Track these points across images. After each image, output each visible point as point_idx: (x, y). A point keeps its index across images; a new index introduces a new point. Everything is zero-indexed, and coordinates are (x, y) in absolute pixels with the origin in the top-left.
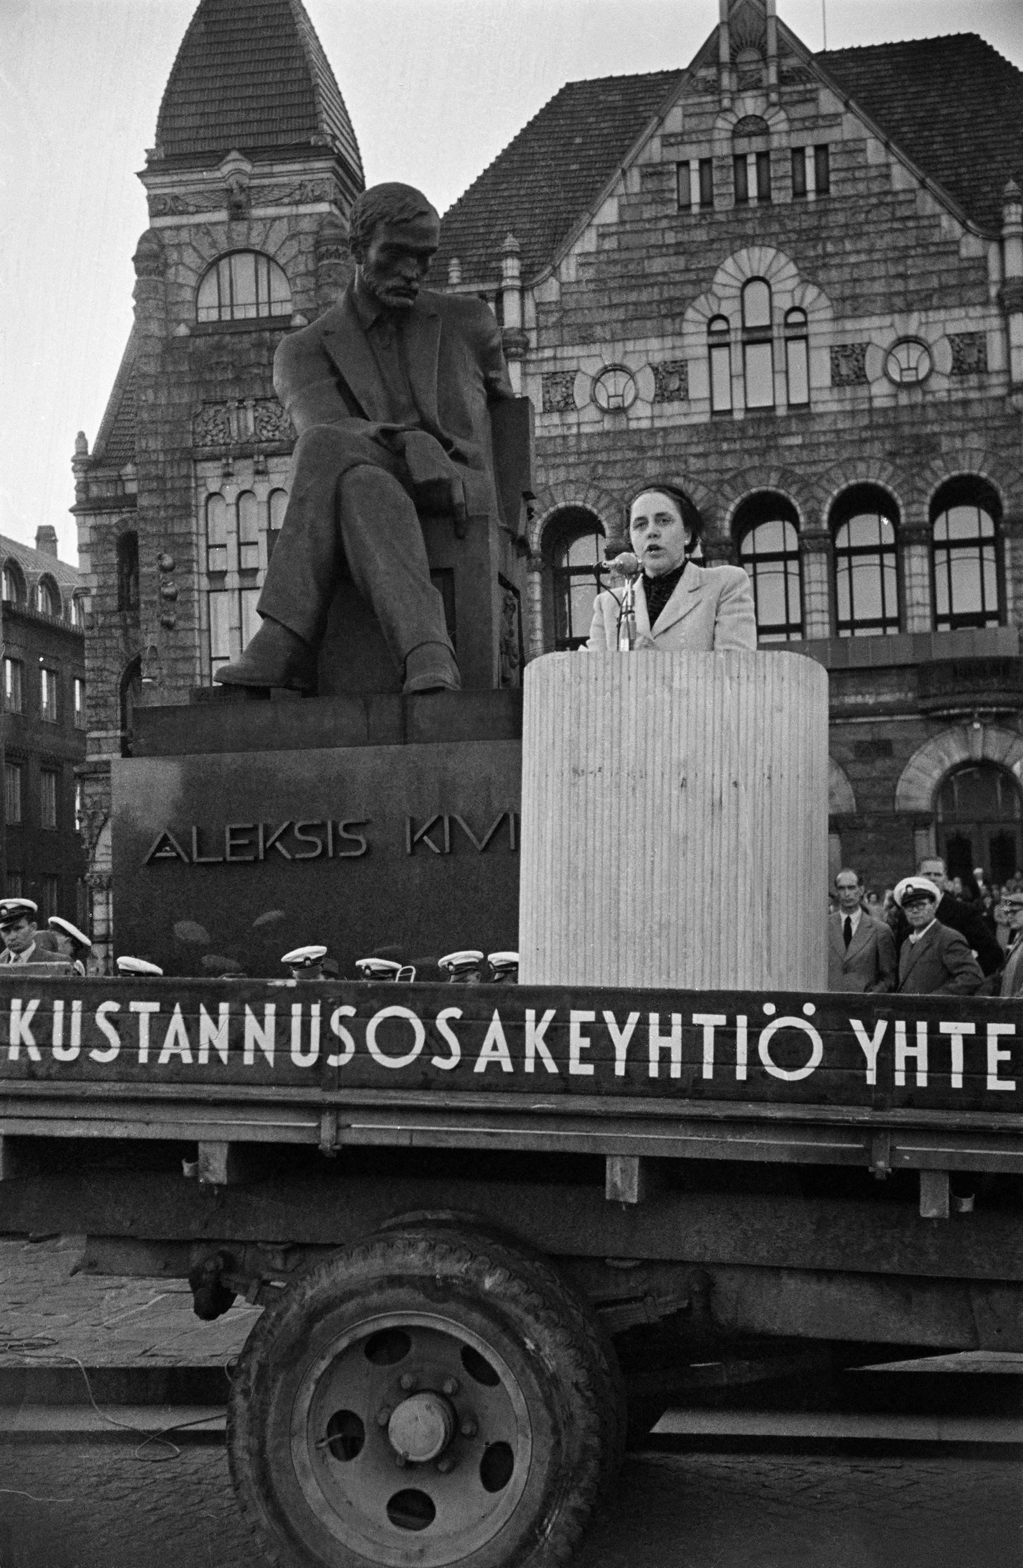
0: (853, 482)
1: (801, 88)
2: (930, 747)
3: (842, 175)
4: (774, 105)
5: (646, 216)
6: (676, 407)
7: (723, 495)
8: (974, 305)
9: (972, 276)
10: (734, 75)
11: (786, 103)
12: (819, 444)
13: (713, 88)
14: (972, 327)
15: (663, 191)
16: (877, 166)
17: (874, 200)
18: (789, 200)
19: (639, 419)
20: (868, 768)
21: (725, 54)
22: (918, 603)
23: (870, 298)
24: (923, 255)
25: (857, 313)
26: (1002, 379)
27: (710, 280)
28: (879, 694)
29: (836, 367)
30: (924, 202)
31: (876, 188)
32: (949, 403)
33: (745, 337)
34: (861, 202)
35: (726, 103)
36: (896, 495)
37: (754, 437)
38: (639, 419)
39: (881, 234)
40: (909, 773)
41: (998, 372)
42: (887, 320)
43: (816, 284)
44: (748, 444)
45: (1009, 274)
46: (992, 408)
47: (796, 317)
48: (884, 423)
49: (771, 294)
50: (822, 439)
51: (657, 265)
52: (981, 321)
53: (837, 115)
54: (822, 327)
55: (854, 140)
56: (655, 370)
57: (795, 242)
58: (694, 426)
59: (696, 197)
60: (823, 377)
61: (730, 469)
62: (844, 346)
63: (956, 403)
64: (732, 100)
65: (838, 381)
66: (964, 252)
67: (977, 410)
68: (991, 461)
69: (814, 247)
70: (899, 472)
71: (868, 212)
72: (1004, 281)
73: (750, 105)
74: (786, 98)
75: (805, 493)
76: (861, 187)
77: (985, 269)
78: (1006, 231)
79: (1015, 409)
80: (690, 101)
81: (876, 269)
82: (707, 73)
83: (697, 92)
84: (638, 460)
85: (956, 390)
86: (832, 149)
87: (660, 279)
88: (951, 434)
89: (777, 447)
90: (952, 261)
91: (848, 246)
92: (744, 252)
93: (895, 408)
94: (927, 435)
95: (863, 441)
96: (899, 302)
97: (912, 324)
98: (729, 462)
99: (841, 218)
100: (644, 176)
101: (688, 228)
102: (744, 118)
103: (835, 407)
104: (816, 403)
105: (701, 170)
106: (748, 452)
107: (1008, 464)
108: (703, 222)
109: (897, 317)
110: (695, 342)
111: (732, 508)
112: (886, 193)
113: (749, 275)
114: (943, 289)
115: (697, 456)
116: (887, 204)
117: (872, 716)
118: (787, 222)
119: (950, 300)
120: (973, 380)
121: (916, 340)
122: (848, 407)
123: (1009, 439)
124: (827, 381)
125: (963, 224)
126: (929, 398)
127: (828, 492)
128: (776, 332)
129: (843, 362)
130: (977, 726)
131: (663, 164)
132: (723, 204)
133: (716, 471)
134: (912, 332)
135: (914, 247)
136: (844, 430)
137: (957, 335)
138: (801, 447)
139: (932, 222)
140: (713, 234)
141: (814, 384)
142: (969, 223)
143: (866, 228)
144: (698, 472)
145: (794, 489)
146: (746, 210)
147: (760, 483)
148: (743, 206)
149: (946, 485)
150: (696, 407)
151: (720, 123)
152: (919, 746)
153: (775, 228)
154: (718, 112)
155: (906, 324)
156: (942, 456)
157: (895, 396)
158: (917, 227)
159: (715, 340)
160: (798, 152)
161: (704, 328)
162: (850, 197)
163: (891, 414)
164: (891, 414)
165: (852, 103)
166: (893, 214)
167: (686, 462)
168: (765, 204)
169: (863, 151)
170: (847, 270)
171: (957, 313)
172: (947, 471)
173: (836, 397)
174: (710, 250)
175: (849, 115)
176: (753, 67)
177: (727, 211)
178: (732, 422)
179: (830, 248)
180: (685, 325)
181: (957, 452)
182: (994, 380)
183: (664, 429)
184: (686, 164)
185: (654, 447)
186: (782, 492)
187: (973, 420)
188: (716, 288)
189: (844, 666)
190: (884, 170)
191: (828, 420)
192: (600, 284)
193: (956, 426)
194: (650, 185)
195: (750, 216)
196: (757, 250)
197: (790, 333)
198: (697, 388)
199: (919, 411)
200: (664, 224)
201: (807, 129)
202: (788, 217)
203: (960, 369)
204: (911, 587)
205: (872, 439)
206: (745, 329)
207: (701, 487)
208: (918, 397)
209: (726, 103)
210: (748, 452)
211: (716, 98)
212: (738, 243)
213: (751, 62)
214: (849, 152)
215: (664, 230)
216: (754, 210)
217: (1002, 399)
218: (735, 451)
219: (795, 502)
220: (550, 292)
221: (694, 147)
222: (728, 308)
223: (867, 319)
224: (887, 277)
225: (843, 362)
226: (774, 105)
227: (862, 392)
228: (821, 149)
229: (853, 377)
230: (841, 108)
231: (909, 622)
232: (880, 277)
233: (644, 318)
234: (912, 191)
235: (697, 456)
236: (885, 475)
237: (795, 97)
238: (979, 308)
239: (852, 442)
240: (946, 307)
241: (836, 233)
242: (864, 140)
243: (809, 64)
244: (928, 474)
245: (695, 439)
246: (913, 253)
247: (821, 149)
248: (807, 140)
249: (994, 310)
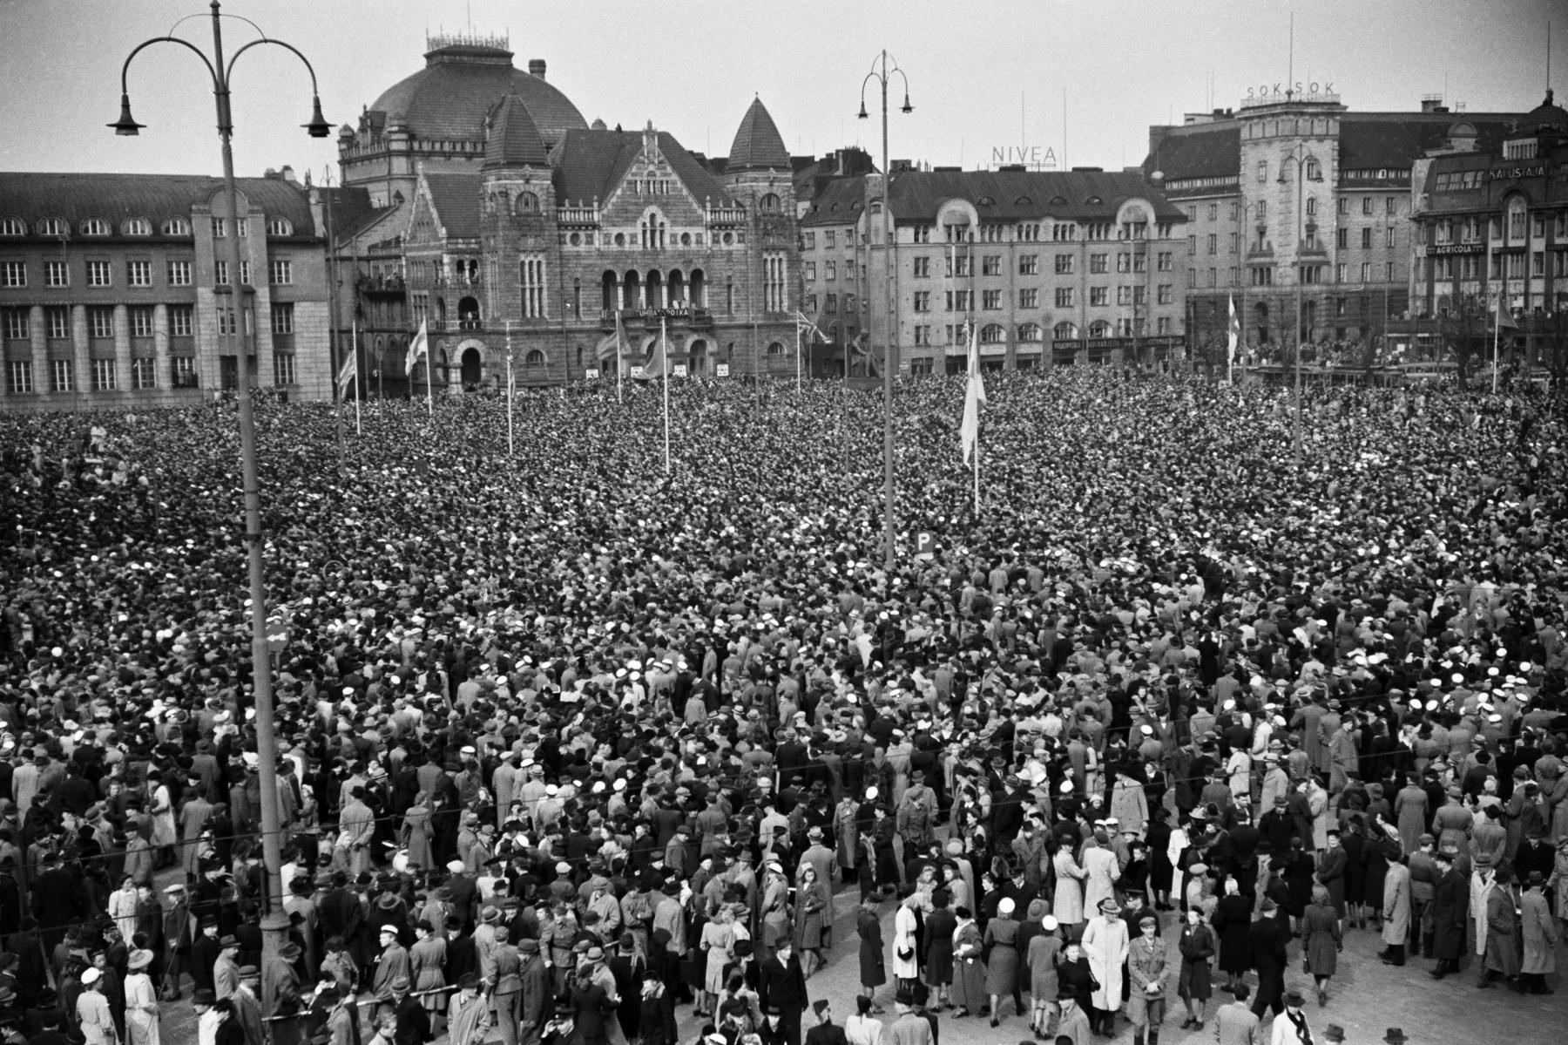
73: (652, 168)
192: (617, 211)
220: (605, 212)
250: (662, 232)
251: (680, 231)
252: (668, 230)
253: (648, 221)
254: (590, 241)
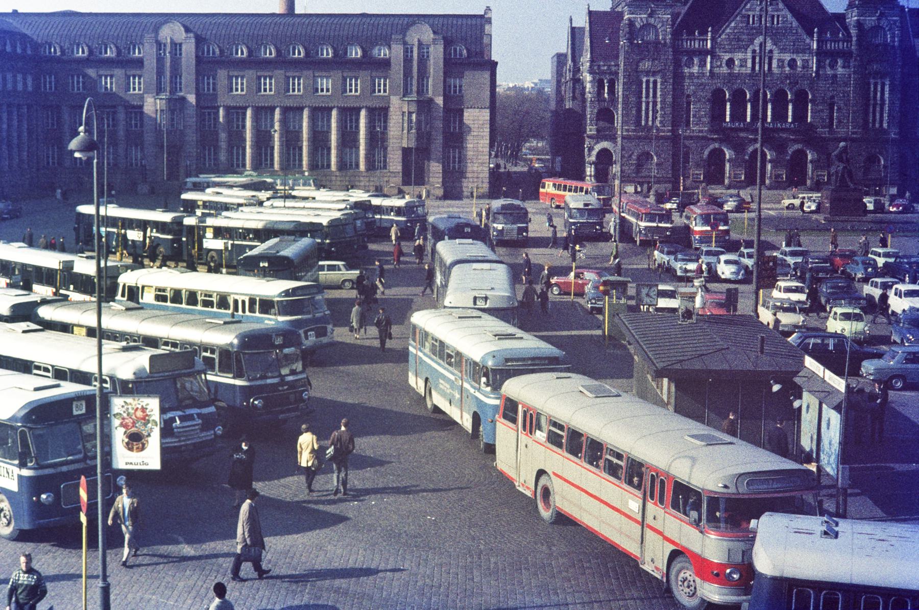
48: (787, 77)
65: (778, 66)
97: (795, 56)
228: (778, 16)
250: (770, 59)
251: (787, 57)
252: (776, 55)
253: (757, 49)
254: (703, 64)
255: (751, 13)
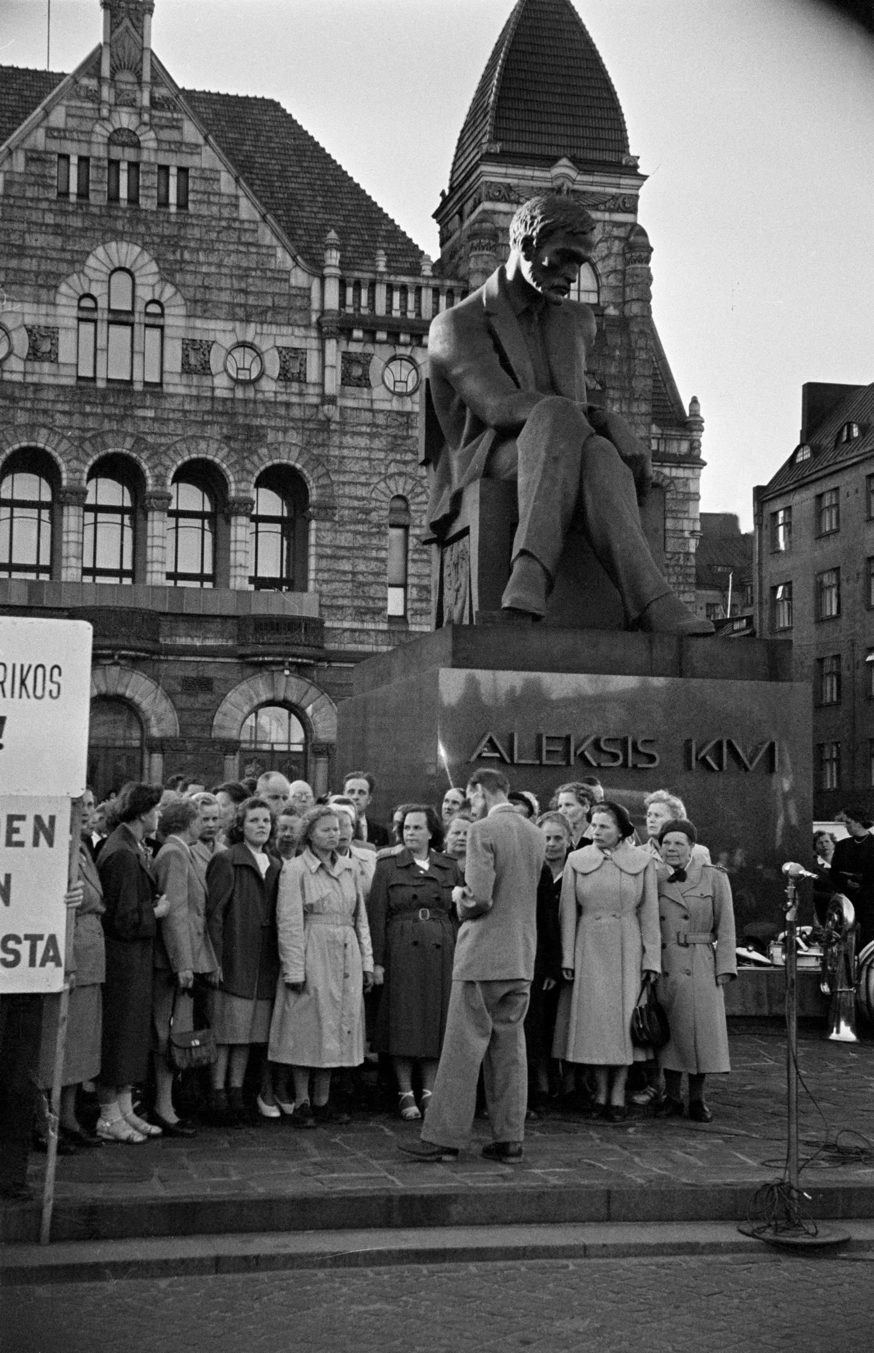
0: (194, 456)
1: (169, 115)
2: (244, 687)
3: (199, 196)
4: (145, 124)
5: (29, 194)
6: (46, 367)
7: (84, 450)
8: (299, 326)
9: (299, 303)
10: (113, 91)
11: (156, 125)
12: (168, 420)
13: (95, 97)
14: (296, 344)
15: (44, 176)
16: (229, 196)
17: (224, 223)
18: (154, 208)
19: (11, 372)
20: (192, 699)
21: (106, 71)
22: (241, 566)
23: (218, 304)
24: (262, 278)
25: (207, 315)
26: (317, 390)
27: (83, 263)
28: (205, 638)
29: (186, 357)
30: (264, 234)
31: (226, 213)
32: (275, 403)
33: (111, 317)
34: (214, 223)
35: (105, 113)
36: (229, 472)
37: (114, 405)
38: (11, 372)
39: (229, 253)
40: (225, 706)
41: (314, 384)
42: (229, 326)
43: (173, 284)
44: (108, 410)
45: (328, 306)
46: (309, 412)
47: (154, 309)
48: (224, 411)
49: (134, 285)
50: (171, 416)
51: (36, 240)
52: (304, 340)
53: (198, 146)
54: (176, 320)
55: (211, 170)
56: (30, 331)
57: (158, 245)
58: (62, 387)
59: (73, 188)
60: (174, 362)
61: (93, 429)
62: (194, 340)
63: (281, 403)
64: (110, 111)
65: (187, 369)
66: (293, 282)
67: (296, 412)
68: (306, 456)
69: (174, 252)
70: (233, 453)
71: (219, 232)
72: (323, 312)
73: (125, 119)
74: (156, 121)
75: (155, 460)
76: (215, 209)
77: (309, 298)
78: (327, 271)
79: (325, 415)
80: (73, 103)
81: (223, 281)
82: (92, 83)
83: (78, 96)
84: (9, 408)
85: (282, 393)
86: (191, 173)
87: (39, 252)
88: (276, 429)
89: (133, 417)
90: (284, 287)
91: (202, 257)
92: (113, 244)
93: (233, 400)
94: (257, 426)
95: (205, 423)
96: (240, 312)
97: (250, 333)
98: (91, 423)
99: (197, 232)
100: (29, 160)
101: (64, 213)
102: (119, 129)
103: (182, 390)
104: (168, 384)
105: (79, 166)
106: (109, 417)
107: (318, 461)
108: (80, 211)
109: (238, 324)
110: (66, 313)
111: (91, 463)
112: (235, 220)
113: (117, 265)
114: (275, 308)
115: (64, 413)
116: (235, 229)
117: (201, 656)
118: (153, 226)
119: (280, 318)
120: (295, 387)
121: (251, 346)
122: (194, 392)
123: (320, 440)
124: (179, 369)
125: (294, 258)
126: (260, 396)
127: (174, 461)
128: (137, 318)
129: (192, 354)
130: (287, 672)
131: (46, 152)
132: (98, 199)
133: (79, 429)
134: (249, 339)
135: (255, 270)
136: (190, 411)
137: (284, 348)
138: (154, 419)
139: (271, 252)
140: (87, 224)
141: (167, 367)
142: (299, 258)
143: (217, 246)
144: (64, 427)
145: (145, 455)
146: (118, 208)
147: (116, 445)
148: (114, 204)
149: (267, 470)
150: (64, 371)
151: (98, 128)
152: (235, 685)
153: (142, 229)
154: (97, 119)
155: (245, 332)
156: (268, 446)
157: (232, 390)
158: (258, 253)
159: (85, 315)
160: (164, 169)
161: (75, 303)
162: (204, 217)
163: (229, 404)
164: (229, 404)
165: (210, 138)
166: (239, 238)
167: (52, 417)
168: (134, 207)
169: (218, 180)
170: (200, 277)
171: (286, 330)
172: (271, 458)
173: (184, 382)
174: (84, 237)
175: (208, 148)
176: (129, 87)
177: (100, 206)
178: (96, 389)
179: (187, 256)
180: (58, 297)
181: (279, 443)
182: (312, 390)
183: (34, 384)
184: (65, 157)
185: (25, 399)
186: (135, 455)
187: (293, 420)
188: (87, 270)
189: (179, 612)
190: (234, 200)
191: (177, 401)
193: (279, 423)
194: (34, 168)
195: (120, 214)
196: (125, 245)
197: (150, 321)
198: (66, 354)
199: (251, 406)
200: (44, 205)
201: (172, 151)
202: (153, 222)
203: (285, 376)
204: (235, 552)
205: (212, 423)
206: (110, 311)
207: (65, 441)
208: (251, 394)
209: (105, 113)
210: (109, 417)
211: (96, 106)
212: (109, 235)
213: (127, 83)
214: (206, 179)
215: (44, 210)
216: (124, 211)
217: (316, 406)
218: (96, 414)
219: (144, 466)
221: (75, 144)
222: (97, 290)
223: (213, 322)
224: (232, 289)
225: (192, 354)
226: (145, 124)
227: (206, 381)
228: (183, 171)
229: (200, 368)
230: (201, 141)
231: (232, 580)
232: (226, 289)
233: (22, 284)
234: (254, 222)
235: (64, 413)
236: (221, 454)
237: (163, 122)
238: (302, 329)
239: (197, 422)
240: (277, 324)
241: (192, 244)
242: (218, 171)
243: (177, 97)
244: (255, 458)
245: (61, 398)
246: (253, 274)
247: (183, 171)
248: (173, 161)
249: (314, 333)
255: (74, 150)
